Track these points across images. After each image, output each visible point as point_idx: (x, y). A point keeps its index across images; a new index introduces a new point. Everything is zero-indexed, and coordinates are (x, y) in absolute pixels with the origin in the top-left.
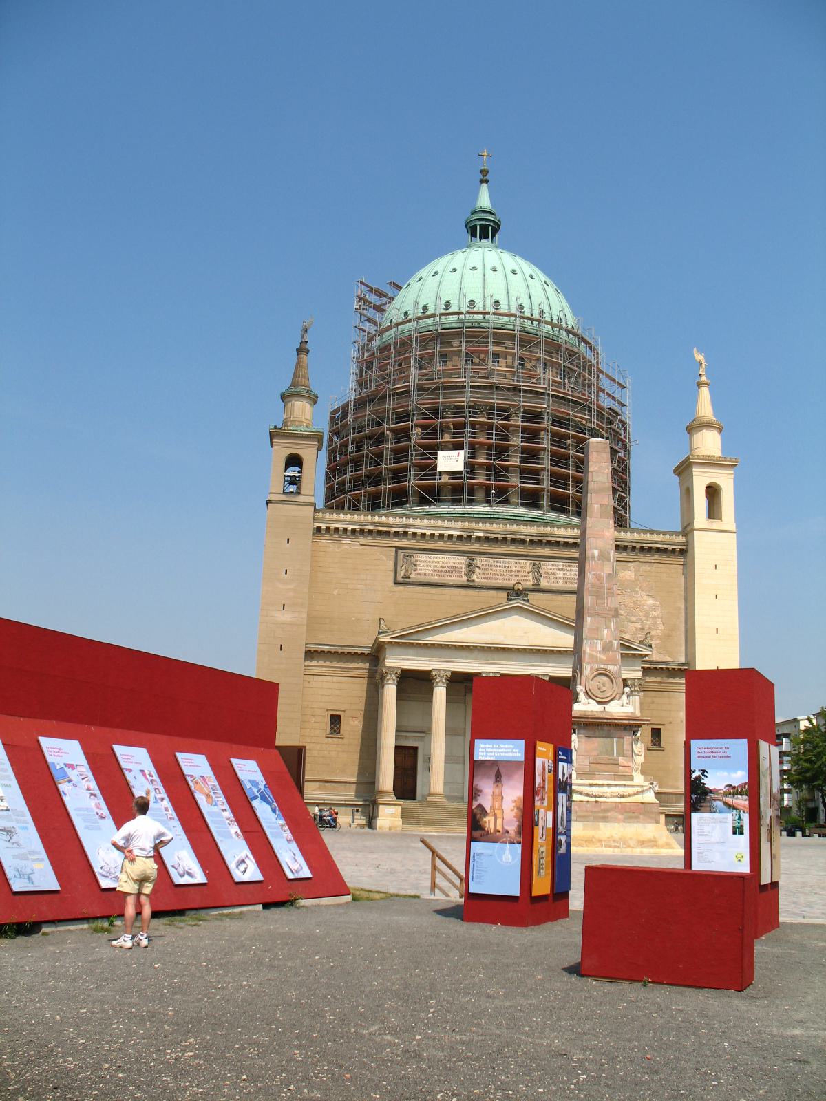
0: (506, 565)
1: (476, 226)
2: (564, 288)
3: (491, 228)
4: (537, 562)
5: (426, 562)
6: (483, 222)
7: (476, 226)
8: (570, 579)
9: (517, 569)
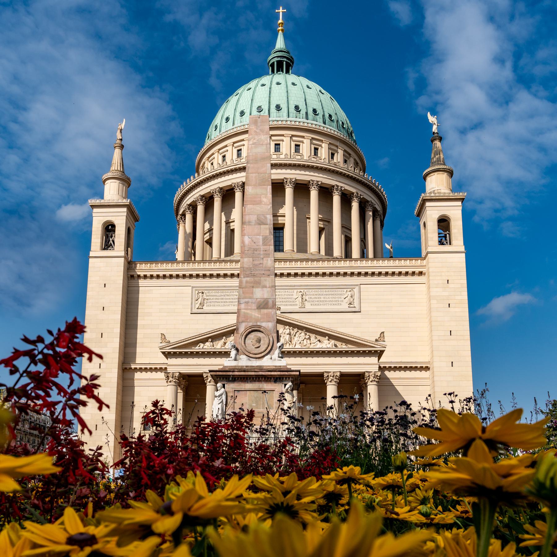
1: (274, 62)
2: (336, 95)
3: (284, 63)
4: (302, 291)
5: (215, 296)
6: (279, 59)
7: (274, 62)
9: (286, 297)
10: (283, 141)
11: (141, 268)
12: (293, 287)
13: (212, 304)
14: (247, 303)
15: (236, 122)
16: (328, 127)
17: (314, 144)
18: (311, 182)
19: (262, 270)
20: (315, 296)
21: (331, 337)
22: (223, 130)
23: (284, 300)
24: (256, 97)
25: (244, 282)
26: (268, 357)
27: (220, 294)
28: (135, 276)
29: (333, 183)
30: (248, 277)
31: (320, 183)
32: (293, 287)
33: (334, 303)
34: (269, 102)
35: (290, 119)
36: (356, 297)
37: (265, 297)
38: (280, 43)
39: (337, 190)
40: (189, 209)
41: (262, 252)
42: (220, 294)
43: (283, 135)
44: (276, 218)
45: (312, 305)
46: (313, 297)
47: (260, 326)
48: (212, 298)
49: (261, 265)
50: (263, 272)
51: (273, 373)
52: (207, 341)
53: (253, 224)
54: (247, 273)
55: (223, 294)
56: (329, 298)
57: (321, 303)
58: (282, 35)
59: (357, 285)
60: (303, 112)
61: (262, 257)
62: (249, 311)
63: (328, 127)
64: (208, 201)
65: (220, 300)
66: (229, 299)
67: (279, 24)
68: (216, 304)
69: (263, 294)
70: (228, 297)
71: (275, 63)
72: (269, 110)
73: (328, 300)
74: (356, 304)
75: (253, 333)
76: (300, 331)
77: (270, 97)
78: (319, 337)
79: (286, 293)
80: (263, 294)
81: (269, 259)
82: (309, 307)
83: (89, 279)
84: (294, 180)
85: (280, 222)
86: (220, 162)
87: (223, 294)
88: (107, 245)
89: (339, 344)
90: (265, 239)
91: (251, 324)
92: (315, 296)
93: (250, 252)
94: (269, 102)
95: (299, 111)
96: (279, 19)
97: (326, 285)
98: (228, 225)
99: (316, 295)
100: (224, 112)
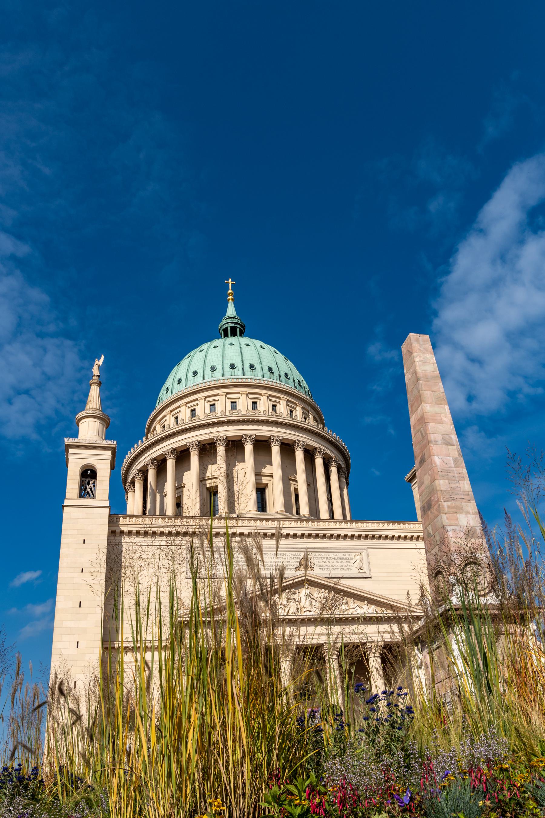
0: (283, 557)
3: (238, 329)
6: (233, 325)
7: (227, 328)
9: (292, 560)
10: (260, 400)
11: (124, 522)
15: (206, 377)
17: (289, 406)
18: (297, 442)
19: (461, 494)
20: (323, 560)
22: (190, 384)
24: (226, 355)
25: (446, 507)
28: (118, 531)
29: (316, 445)
31: (305, 444)
33: (343, 567)
34: (242, 361)
36: (365, 561)
38: (231, 310)
39: (320, 452)
40: (153, 463)
41: (456, 475)
43: (260, 394)
44: (258, 477)
46: (321, 561)
49: (459, 489)
50: (462, 497)
53: (440, 443)
56: (337, 562)
57: (331, 568)
58: (233, 304)
59: (365, 549)
60: (276, 374)
61: (457, 479)
64: (182, 456)
67: (229, 294)
71: (229, 329)
72: (243, 368)
73: (337, 564)
74: (365, 569)
77: (242, 356)
78: (359, 603)
79: (293, 556)
81: (465, 482)
83: (63, 533)
84: (281, 438)
85: (263, 482)
86: (208, 411)
88: (85, 492)
89: (379, 609)
90: (455, 460)
92: (323, 560)
93: (443, 473)
94: (242, 361)
95: (273, 373)
96: (229, 289)
97: (334, 549)
98: (203, 482)
99: (324, 558)
100: (189, 366)
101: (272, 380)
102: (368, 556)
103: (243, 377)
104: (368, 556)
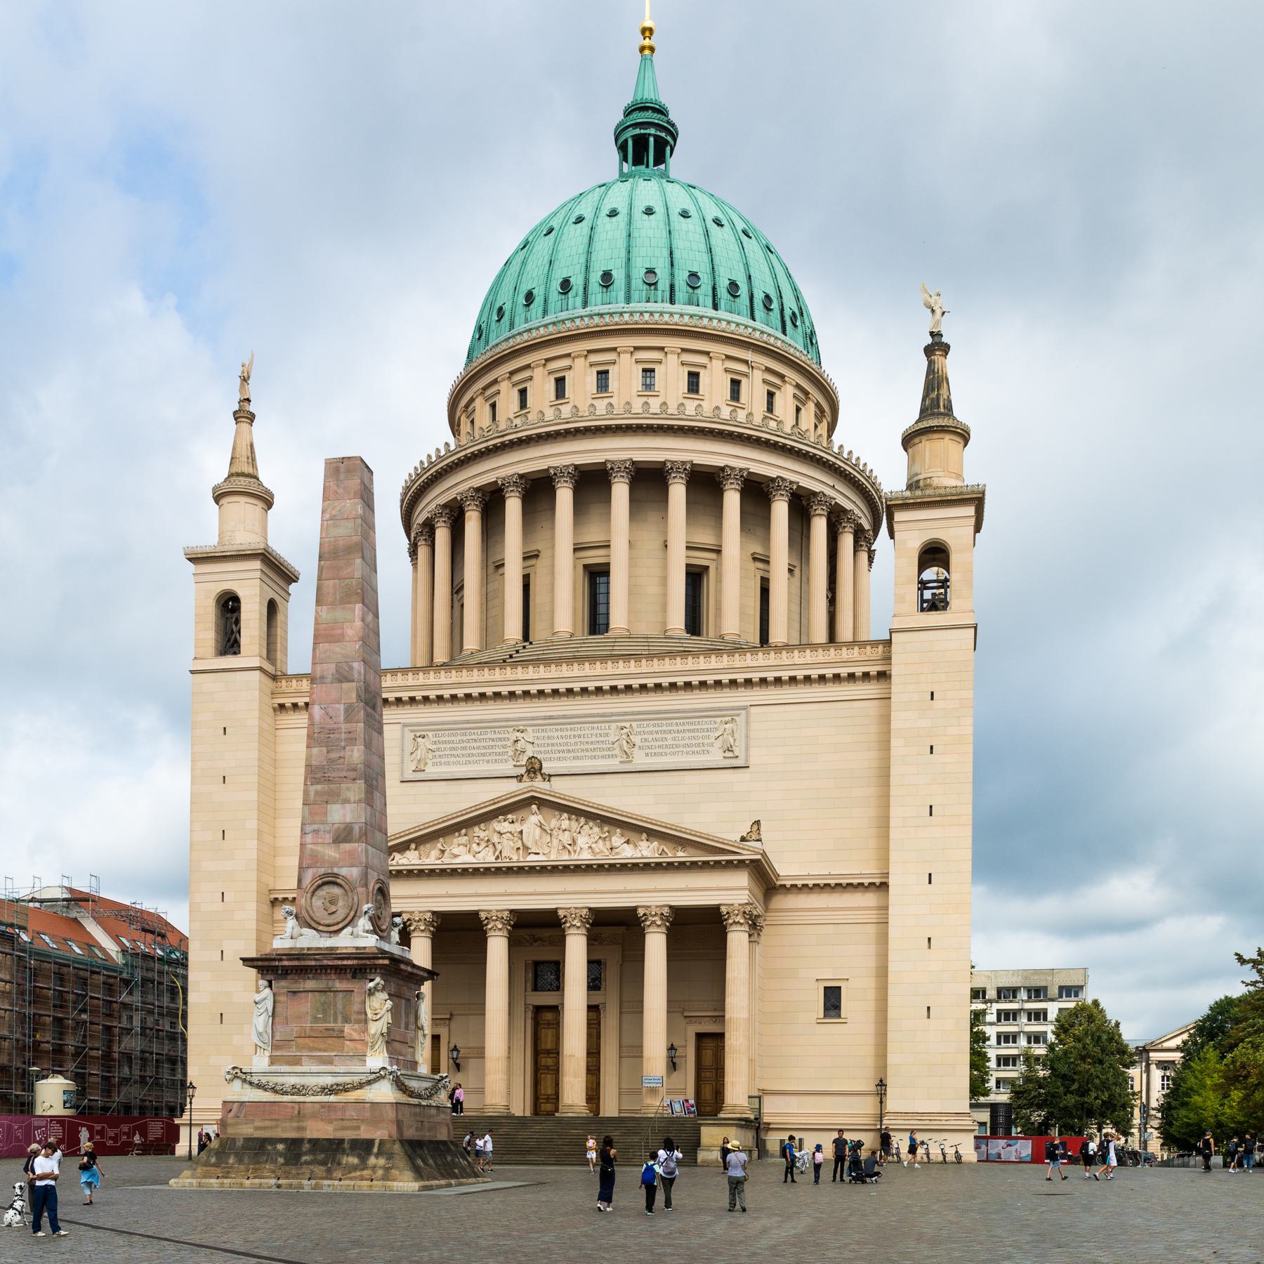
5: (449, 742)
8: (685, 745)
9: (594, 739)
12: (605, 718)
13: (443, 760)
14: (316, 832)
16: (729, 316)
20: (655, 736)
21: (652, 834)
23: (590, 746)
26: (349, 929)
27: (459, 738)
30: (318, 783)
32: (605, 718)
33: (694, 749)
35: (634, 306)
37: (348, 820)
42: (459, 738)
45: (647, 755)
46: (650, 737)
47: (336, 875)
48: (443, 746)
51: (345, 962)
52: (408, 848)
54: (318, 776)
55: (464, 738)
56: (683, 739)
57: (668, 751)
59: (745, 708)
62: (319, 848)
63: (729, 316)
65: (459, 752)
66: (478, 748)
68: (453, 759)
69: (344, 816)
70: (476, 745)
75: (325, 887)
76: (591, 824)
80: (344, 816)
82: (640, 760)
87: (464, 738)
91: (322, 871)
92: (655, 736)
97: (678, 711)
99: (657, 732)
101: (651, 306)
102: (747, 723)
103: (582, 312)
104: (747, 723)
